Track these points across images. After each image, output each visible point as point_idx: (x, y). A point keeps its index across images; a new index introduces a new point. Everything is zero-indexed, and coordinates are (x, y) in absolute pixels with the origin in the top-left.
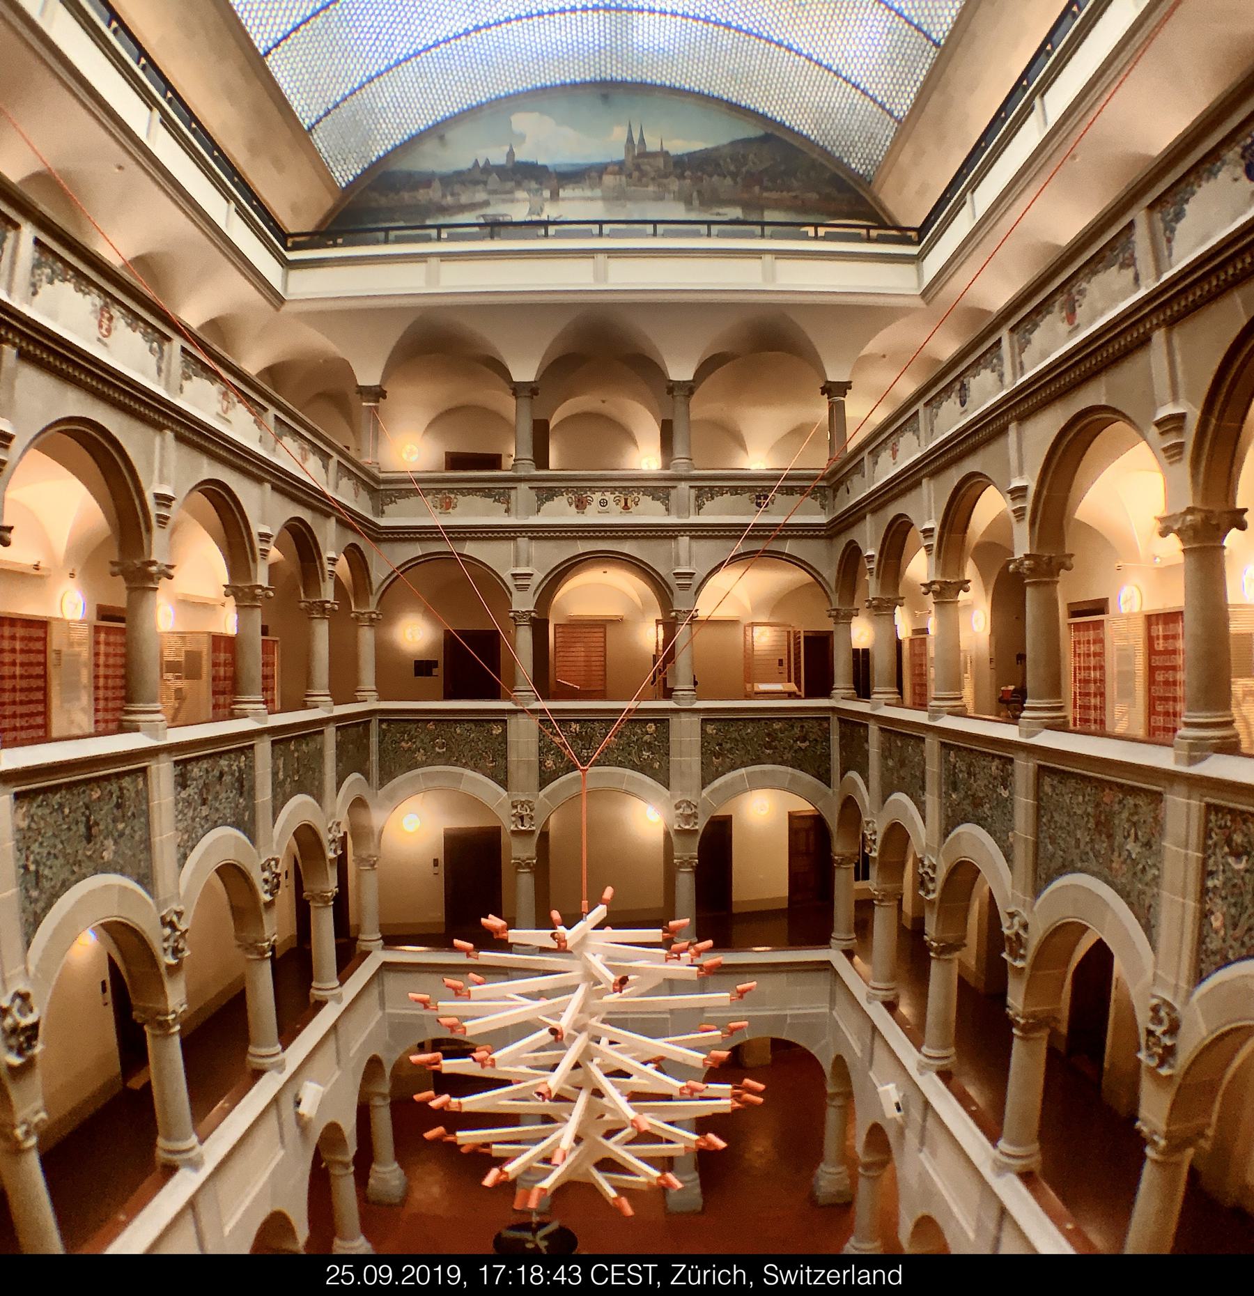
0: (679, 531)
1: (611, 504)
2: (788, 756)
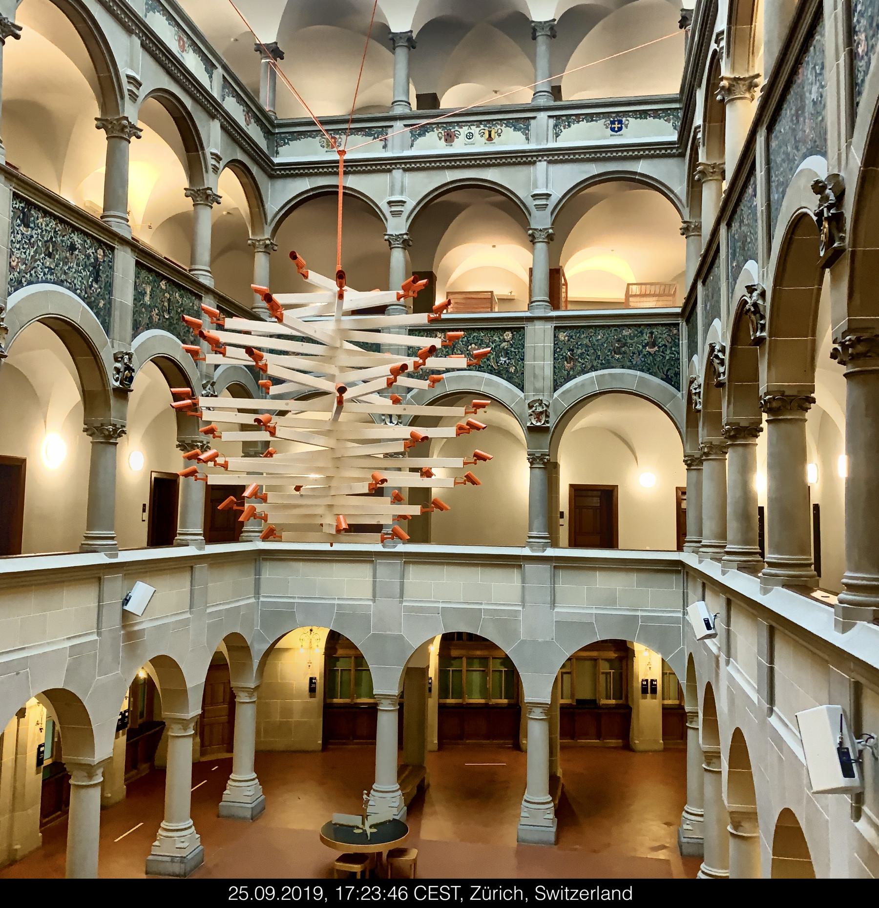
0: (537, 156)
1: (477, 136)
2: (636, 360)
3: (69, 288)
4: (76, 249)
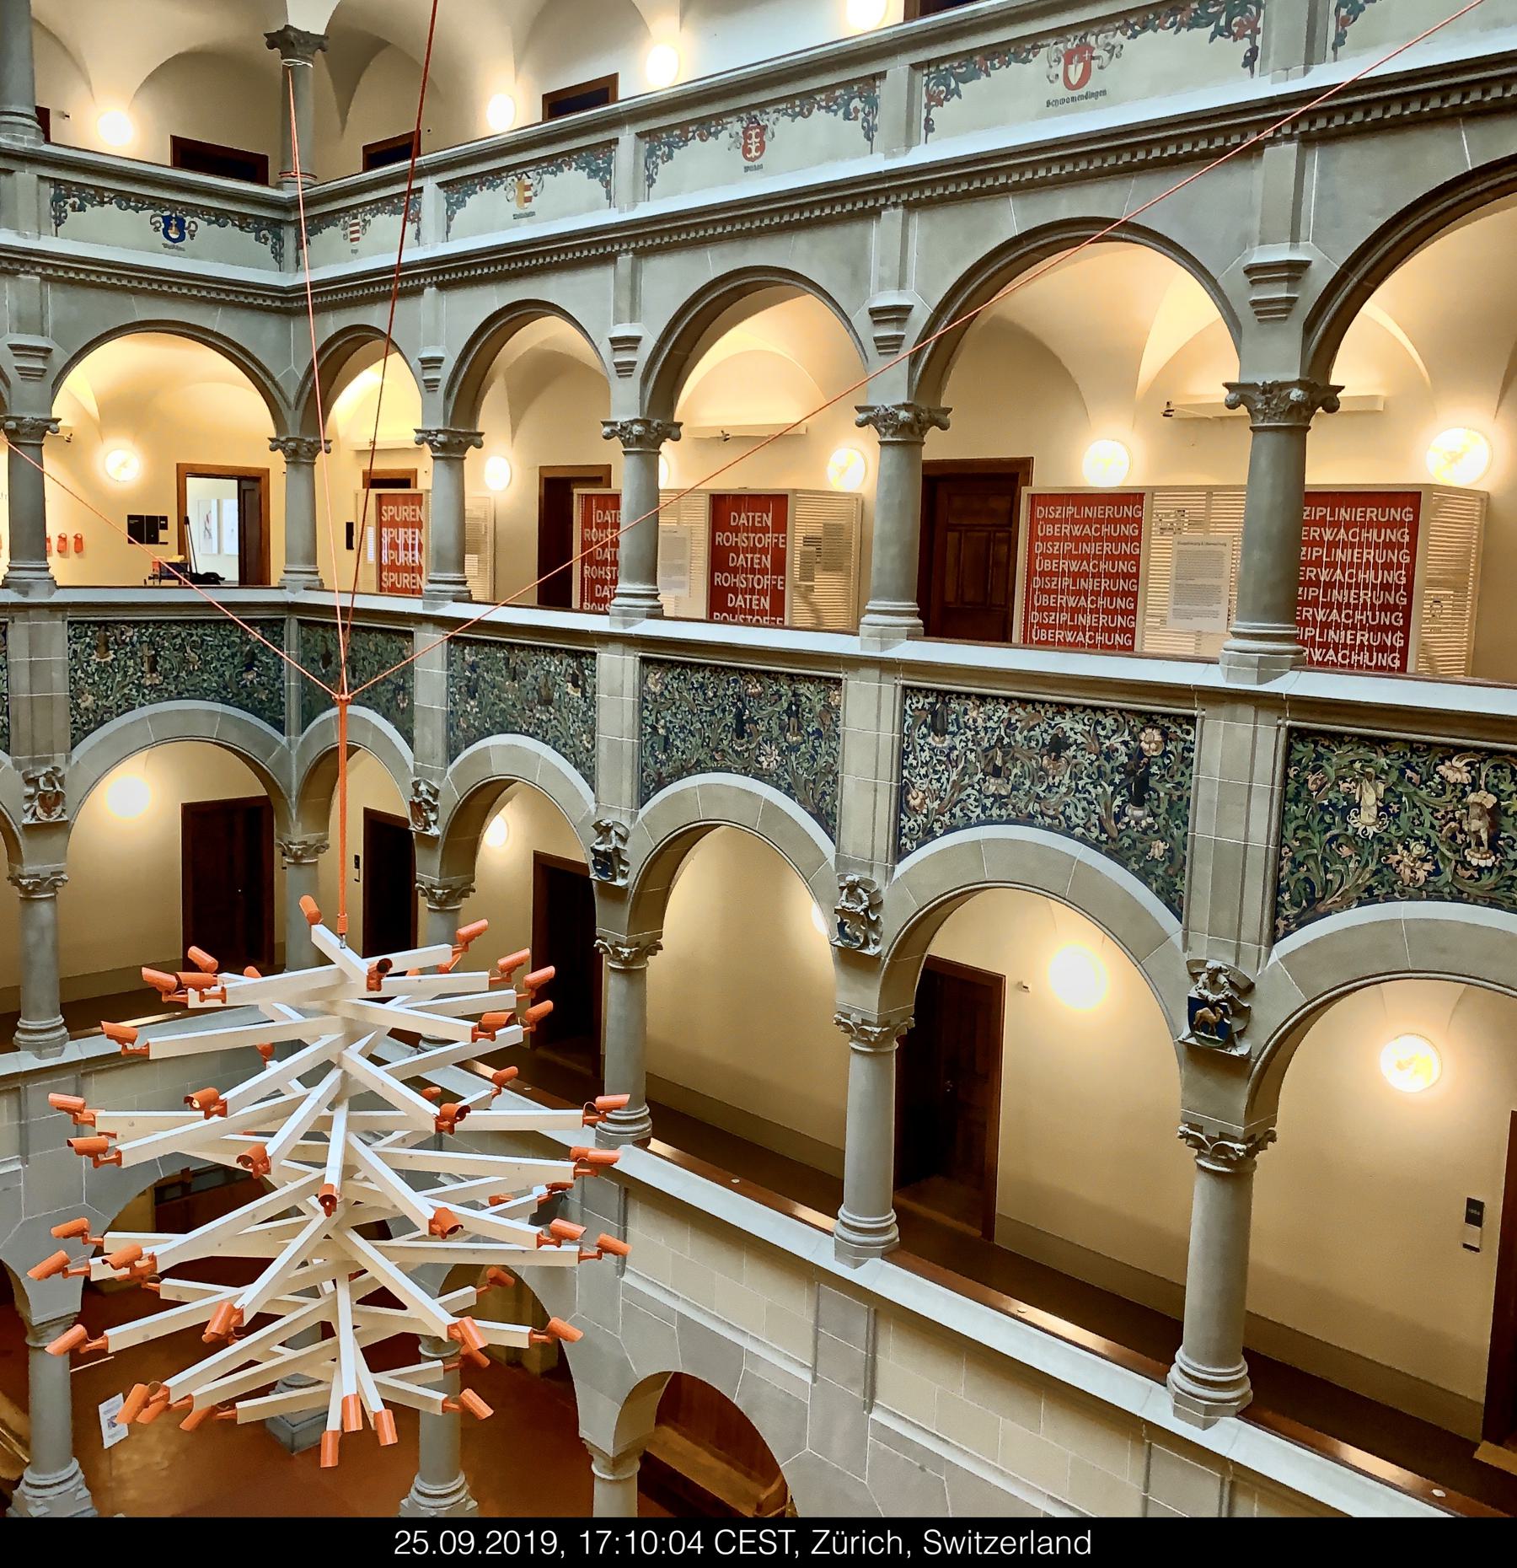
3: (1050, 828)
4: (1069, 747)
